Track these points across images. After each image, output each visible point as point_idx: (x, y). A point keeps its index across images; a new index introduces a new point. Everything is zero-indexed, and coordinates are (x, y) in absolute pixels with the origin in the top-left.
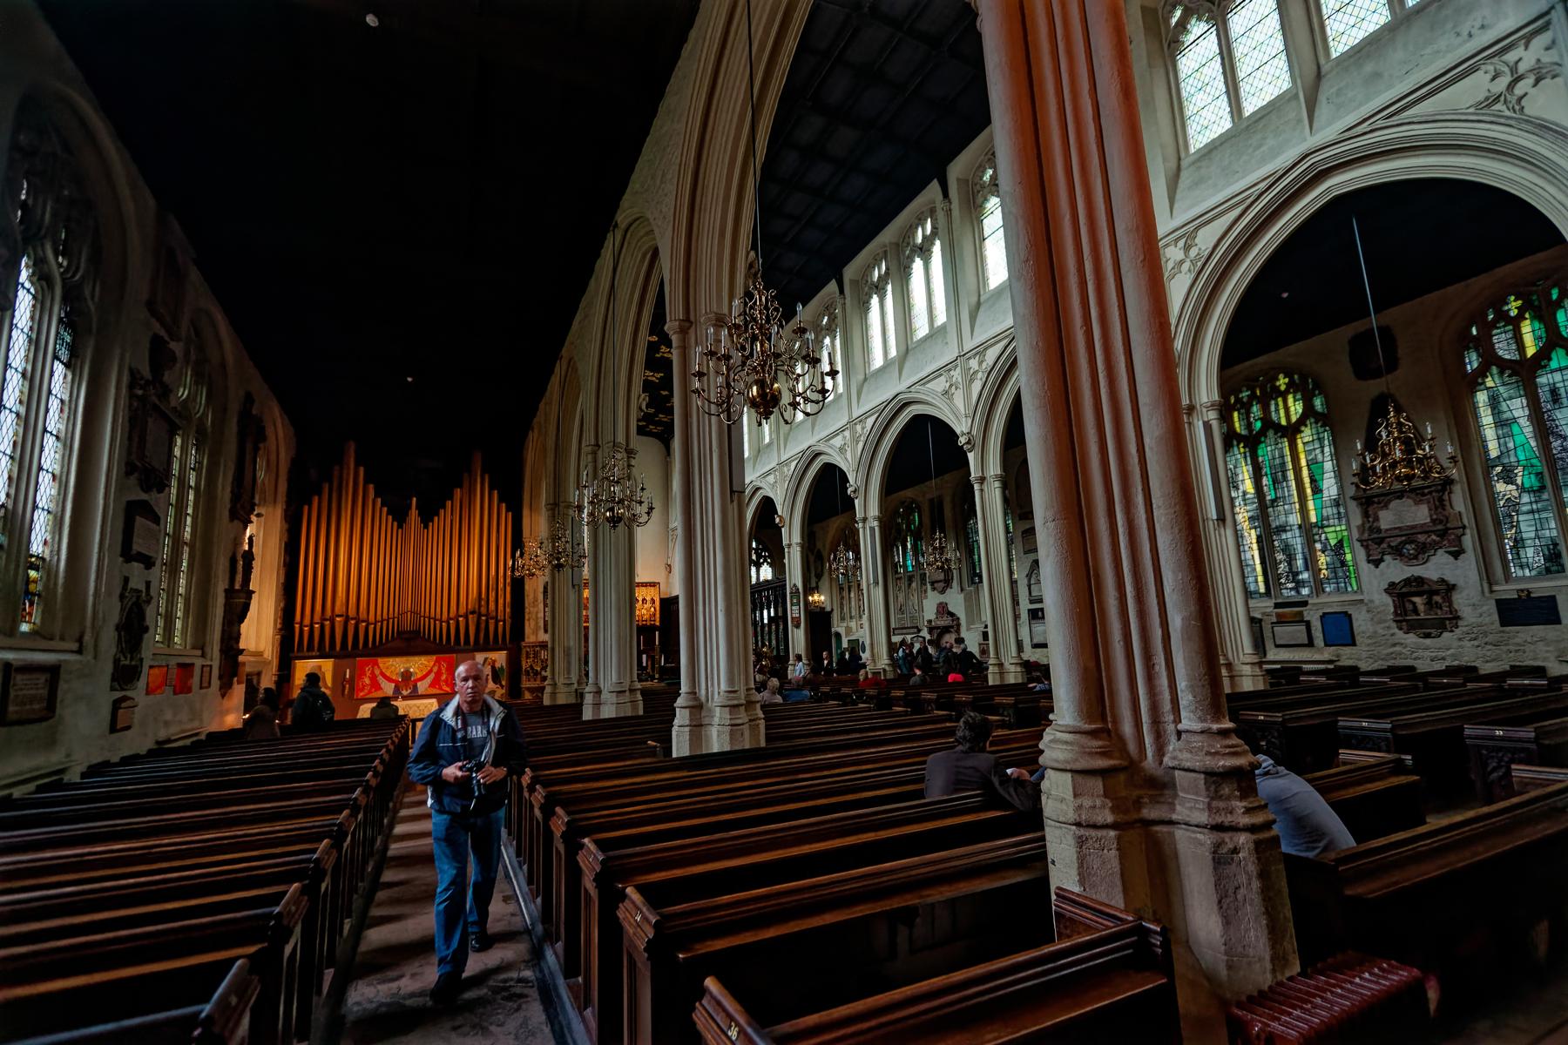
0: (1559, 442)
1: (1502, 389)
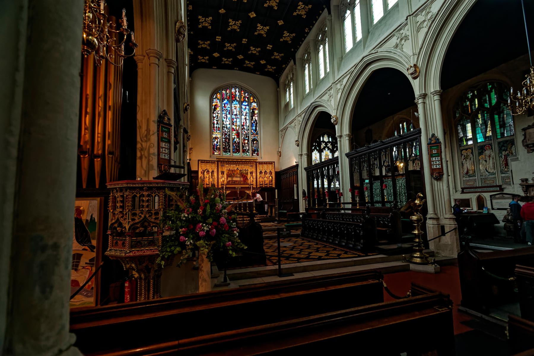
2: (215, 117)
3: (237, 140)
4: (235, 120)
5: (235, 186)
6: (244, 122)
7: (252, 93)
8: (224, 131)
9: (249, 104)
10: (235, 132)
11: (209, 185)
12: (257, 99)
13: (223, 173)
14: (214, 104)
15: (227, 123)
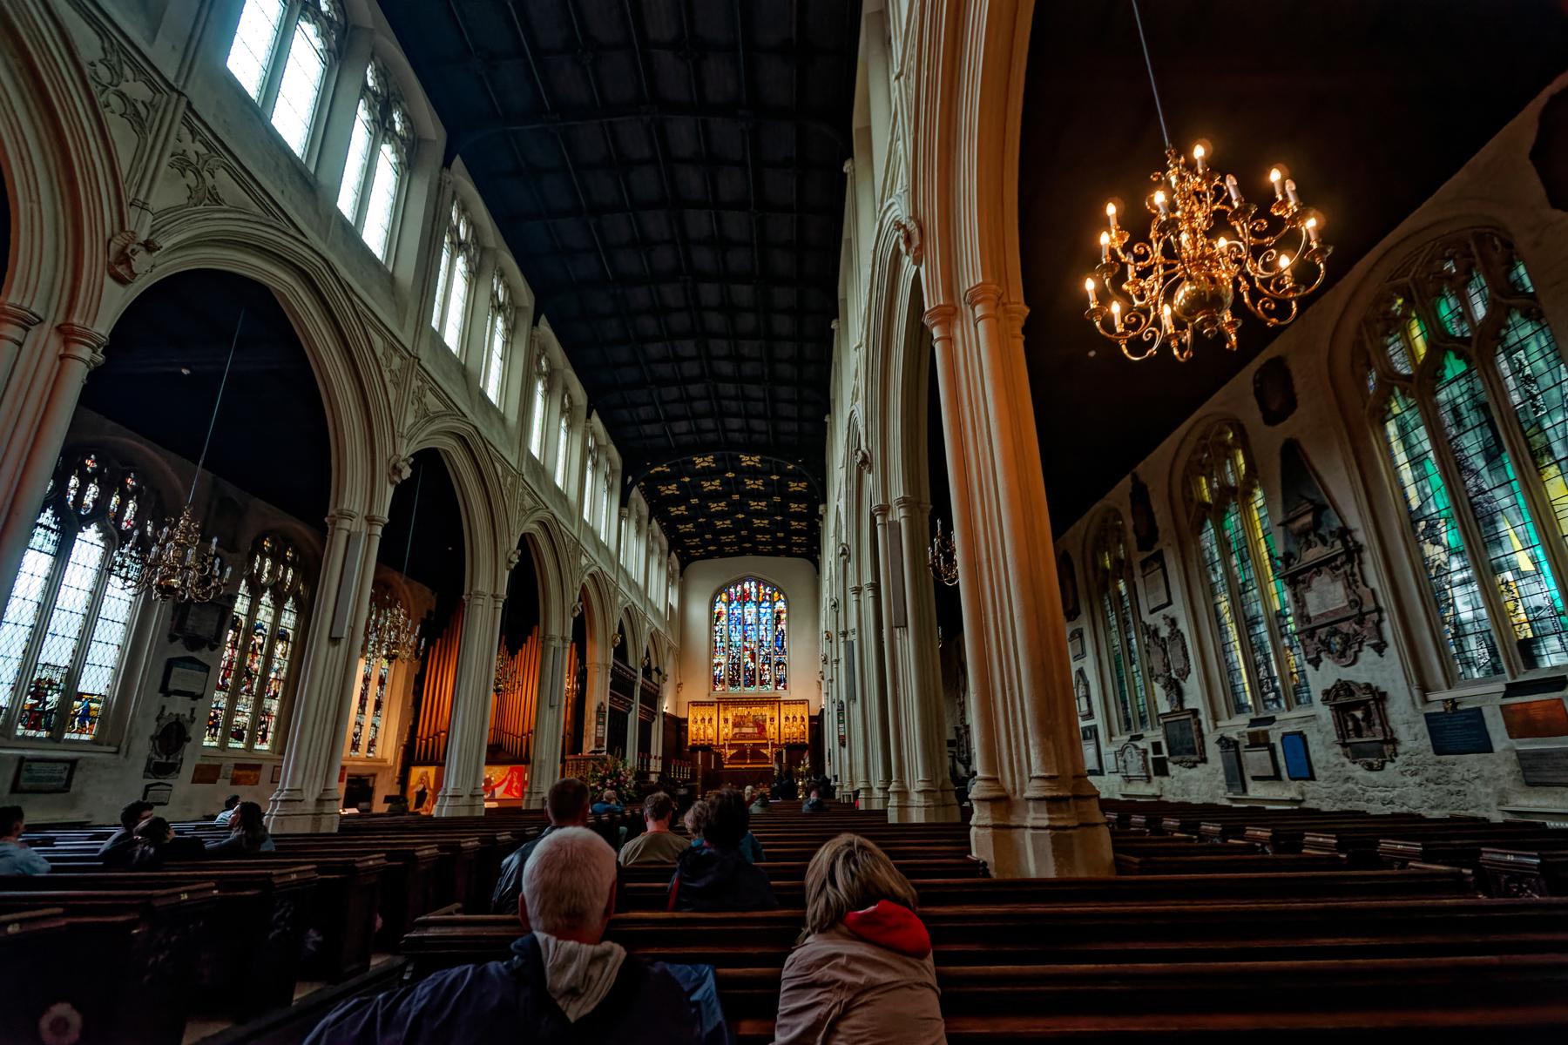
0: (1473, 480)
1: (1407, 415)
3: (751, 665)
9: (773, 604)
12: (785, 596)
13: (726, 721)
14: (717, 611)
15: (736, 637)
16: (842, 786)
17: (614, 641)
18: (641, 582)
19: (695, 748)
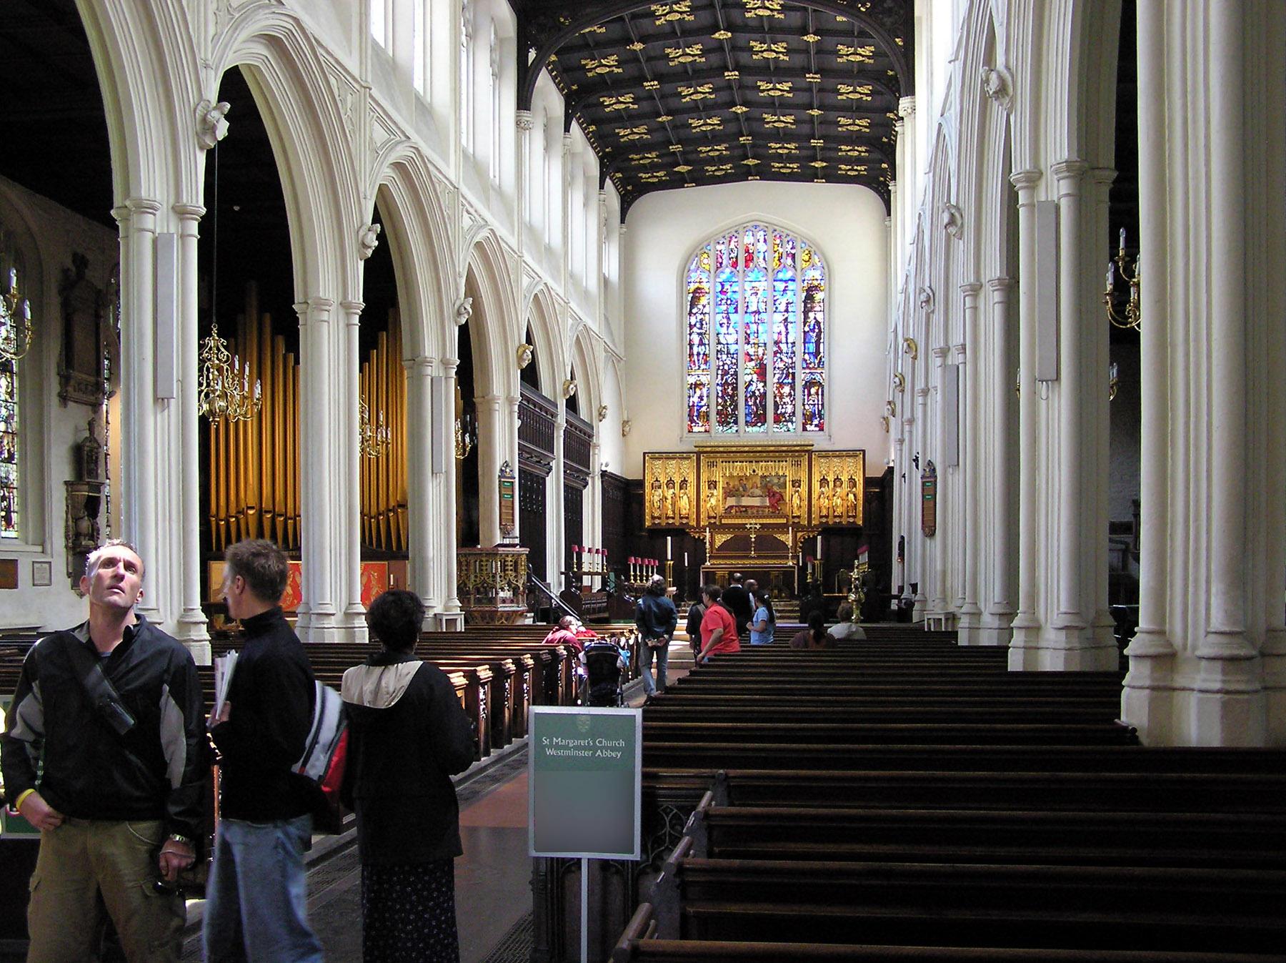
2: (695, 325)
3: (757, 387)
4: (754, 327)
5: (747, 521)
6: (780, 333)
7: (805, 241)
8: (721, 363)
10: (753, 364)
11: (673, 518)
13: (712, 484)
14: (692, 287)
16: (924, 601)
17: (520, 359)
18: (556, 240)
19: (659, 533)
